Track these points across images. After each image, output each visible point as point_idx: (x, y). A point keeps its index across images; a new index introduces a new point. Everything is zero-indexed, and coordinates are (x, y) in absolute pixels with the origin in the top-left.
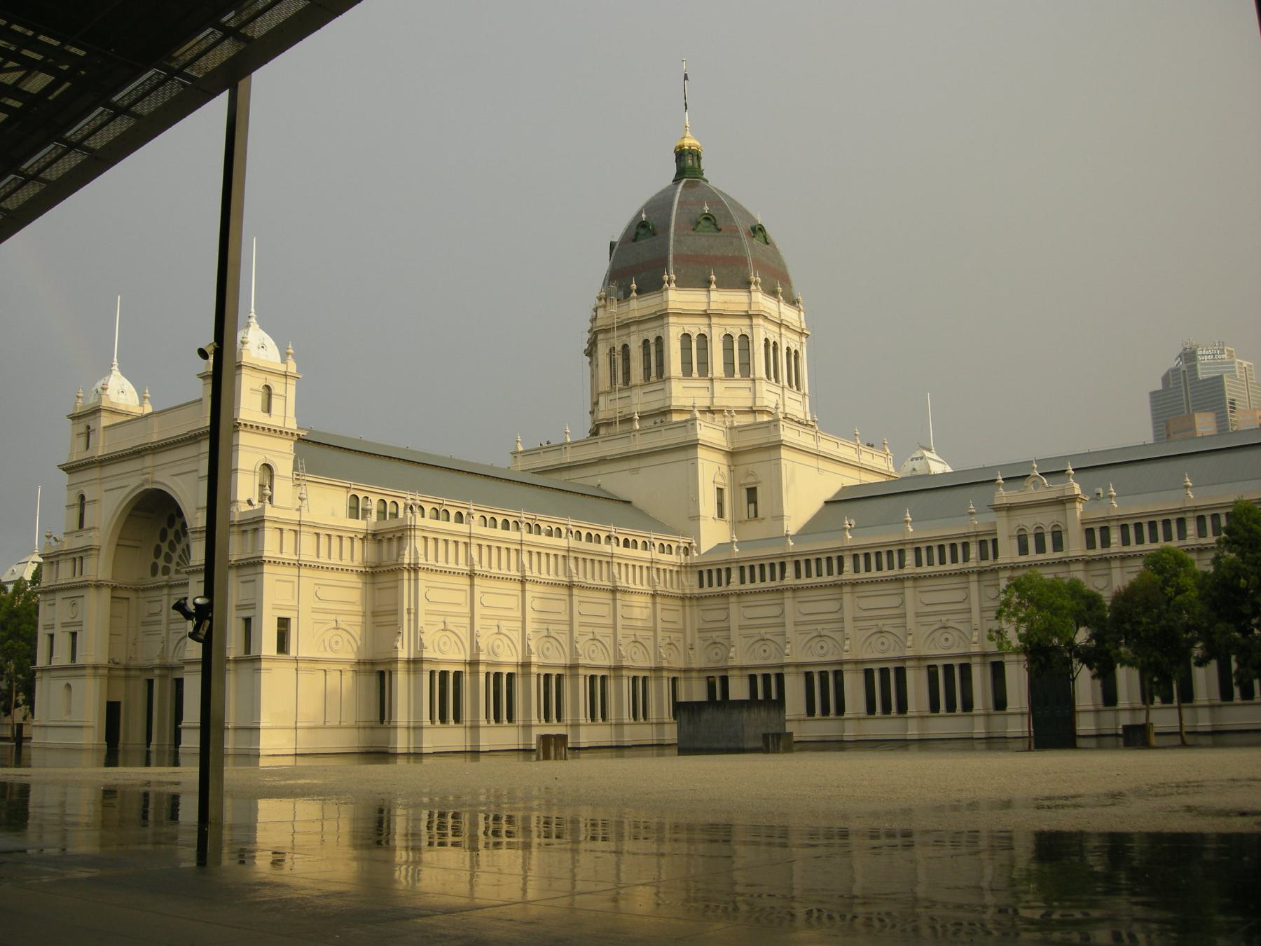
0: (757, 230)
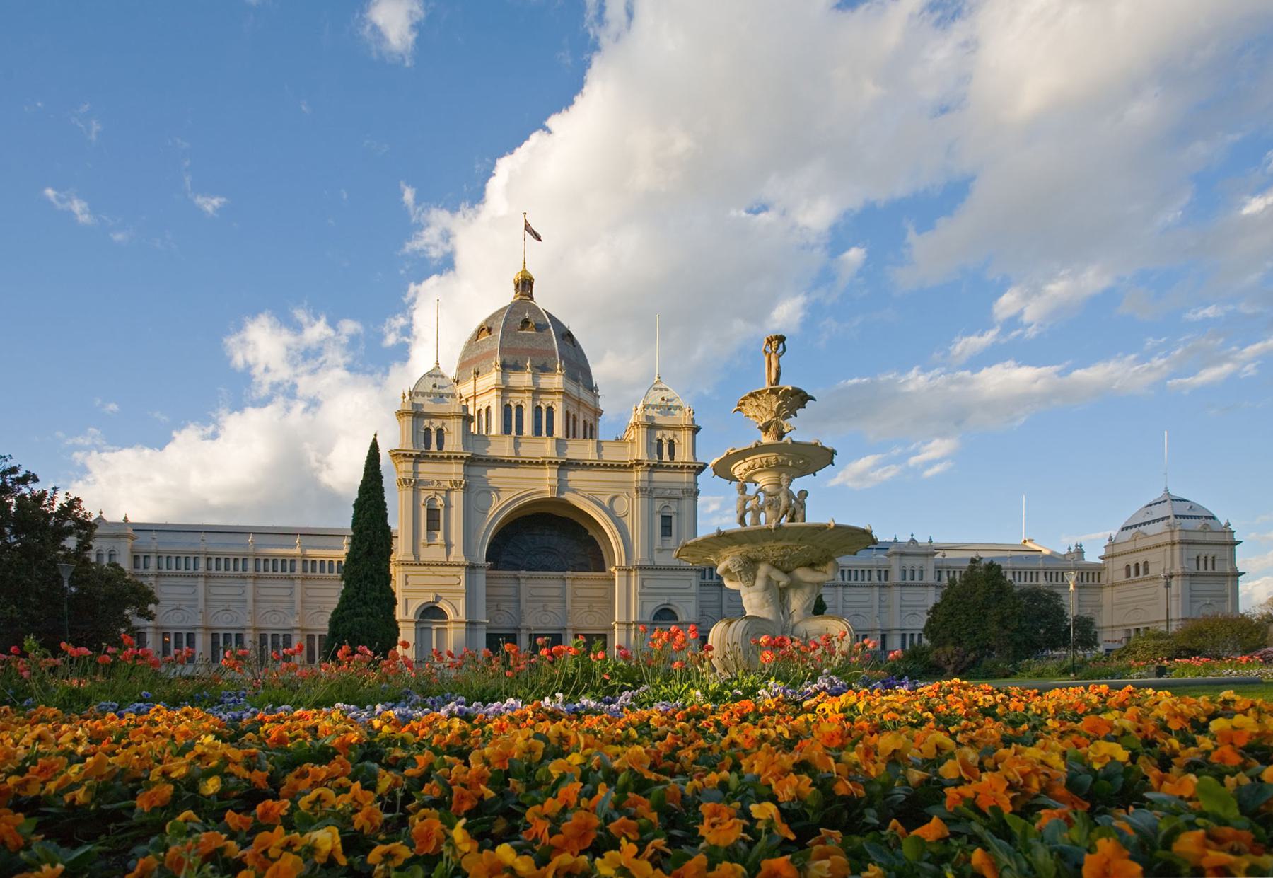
0: (566, 336)
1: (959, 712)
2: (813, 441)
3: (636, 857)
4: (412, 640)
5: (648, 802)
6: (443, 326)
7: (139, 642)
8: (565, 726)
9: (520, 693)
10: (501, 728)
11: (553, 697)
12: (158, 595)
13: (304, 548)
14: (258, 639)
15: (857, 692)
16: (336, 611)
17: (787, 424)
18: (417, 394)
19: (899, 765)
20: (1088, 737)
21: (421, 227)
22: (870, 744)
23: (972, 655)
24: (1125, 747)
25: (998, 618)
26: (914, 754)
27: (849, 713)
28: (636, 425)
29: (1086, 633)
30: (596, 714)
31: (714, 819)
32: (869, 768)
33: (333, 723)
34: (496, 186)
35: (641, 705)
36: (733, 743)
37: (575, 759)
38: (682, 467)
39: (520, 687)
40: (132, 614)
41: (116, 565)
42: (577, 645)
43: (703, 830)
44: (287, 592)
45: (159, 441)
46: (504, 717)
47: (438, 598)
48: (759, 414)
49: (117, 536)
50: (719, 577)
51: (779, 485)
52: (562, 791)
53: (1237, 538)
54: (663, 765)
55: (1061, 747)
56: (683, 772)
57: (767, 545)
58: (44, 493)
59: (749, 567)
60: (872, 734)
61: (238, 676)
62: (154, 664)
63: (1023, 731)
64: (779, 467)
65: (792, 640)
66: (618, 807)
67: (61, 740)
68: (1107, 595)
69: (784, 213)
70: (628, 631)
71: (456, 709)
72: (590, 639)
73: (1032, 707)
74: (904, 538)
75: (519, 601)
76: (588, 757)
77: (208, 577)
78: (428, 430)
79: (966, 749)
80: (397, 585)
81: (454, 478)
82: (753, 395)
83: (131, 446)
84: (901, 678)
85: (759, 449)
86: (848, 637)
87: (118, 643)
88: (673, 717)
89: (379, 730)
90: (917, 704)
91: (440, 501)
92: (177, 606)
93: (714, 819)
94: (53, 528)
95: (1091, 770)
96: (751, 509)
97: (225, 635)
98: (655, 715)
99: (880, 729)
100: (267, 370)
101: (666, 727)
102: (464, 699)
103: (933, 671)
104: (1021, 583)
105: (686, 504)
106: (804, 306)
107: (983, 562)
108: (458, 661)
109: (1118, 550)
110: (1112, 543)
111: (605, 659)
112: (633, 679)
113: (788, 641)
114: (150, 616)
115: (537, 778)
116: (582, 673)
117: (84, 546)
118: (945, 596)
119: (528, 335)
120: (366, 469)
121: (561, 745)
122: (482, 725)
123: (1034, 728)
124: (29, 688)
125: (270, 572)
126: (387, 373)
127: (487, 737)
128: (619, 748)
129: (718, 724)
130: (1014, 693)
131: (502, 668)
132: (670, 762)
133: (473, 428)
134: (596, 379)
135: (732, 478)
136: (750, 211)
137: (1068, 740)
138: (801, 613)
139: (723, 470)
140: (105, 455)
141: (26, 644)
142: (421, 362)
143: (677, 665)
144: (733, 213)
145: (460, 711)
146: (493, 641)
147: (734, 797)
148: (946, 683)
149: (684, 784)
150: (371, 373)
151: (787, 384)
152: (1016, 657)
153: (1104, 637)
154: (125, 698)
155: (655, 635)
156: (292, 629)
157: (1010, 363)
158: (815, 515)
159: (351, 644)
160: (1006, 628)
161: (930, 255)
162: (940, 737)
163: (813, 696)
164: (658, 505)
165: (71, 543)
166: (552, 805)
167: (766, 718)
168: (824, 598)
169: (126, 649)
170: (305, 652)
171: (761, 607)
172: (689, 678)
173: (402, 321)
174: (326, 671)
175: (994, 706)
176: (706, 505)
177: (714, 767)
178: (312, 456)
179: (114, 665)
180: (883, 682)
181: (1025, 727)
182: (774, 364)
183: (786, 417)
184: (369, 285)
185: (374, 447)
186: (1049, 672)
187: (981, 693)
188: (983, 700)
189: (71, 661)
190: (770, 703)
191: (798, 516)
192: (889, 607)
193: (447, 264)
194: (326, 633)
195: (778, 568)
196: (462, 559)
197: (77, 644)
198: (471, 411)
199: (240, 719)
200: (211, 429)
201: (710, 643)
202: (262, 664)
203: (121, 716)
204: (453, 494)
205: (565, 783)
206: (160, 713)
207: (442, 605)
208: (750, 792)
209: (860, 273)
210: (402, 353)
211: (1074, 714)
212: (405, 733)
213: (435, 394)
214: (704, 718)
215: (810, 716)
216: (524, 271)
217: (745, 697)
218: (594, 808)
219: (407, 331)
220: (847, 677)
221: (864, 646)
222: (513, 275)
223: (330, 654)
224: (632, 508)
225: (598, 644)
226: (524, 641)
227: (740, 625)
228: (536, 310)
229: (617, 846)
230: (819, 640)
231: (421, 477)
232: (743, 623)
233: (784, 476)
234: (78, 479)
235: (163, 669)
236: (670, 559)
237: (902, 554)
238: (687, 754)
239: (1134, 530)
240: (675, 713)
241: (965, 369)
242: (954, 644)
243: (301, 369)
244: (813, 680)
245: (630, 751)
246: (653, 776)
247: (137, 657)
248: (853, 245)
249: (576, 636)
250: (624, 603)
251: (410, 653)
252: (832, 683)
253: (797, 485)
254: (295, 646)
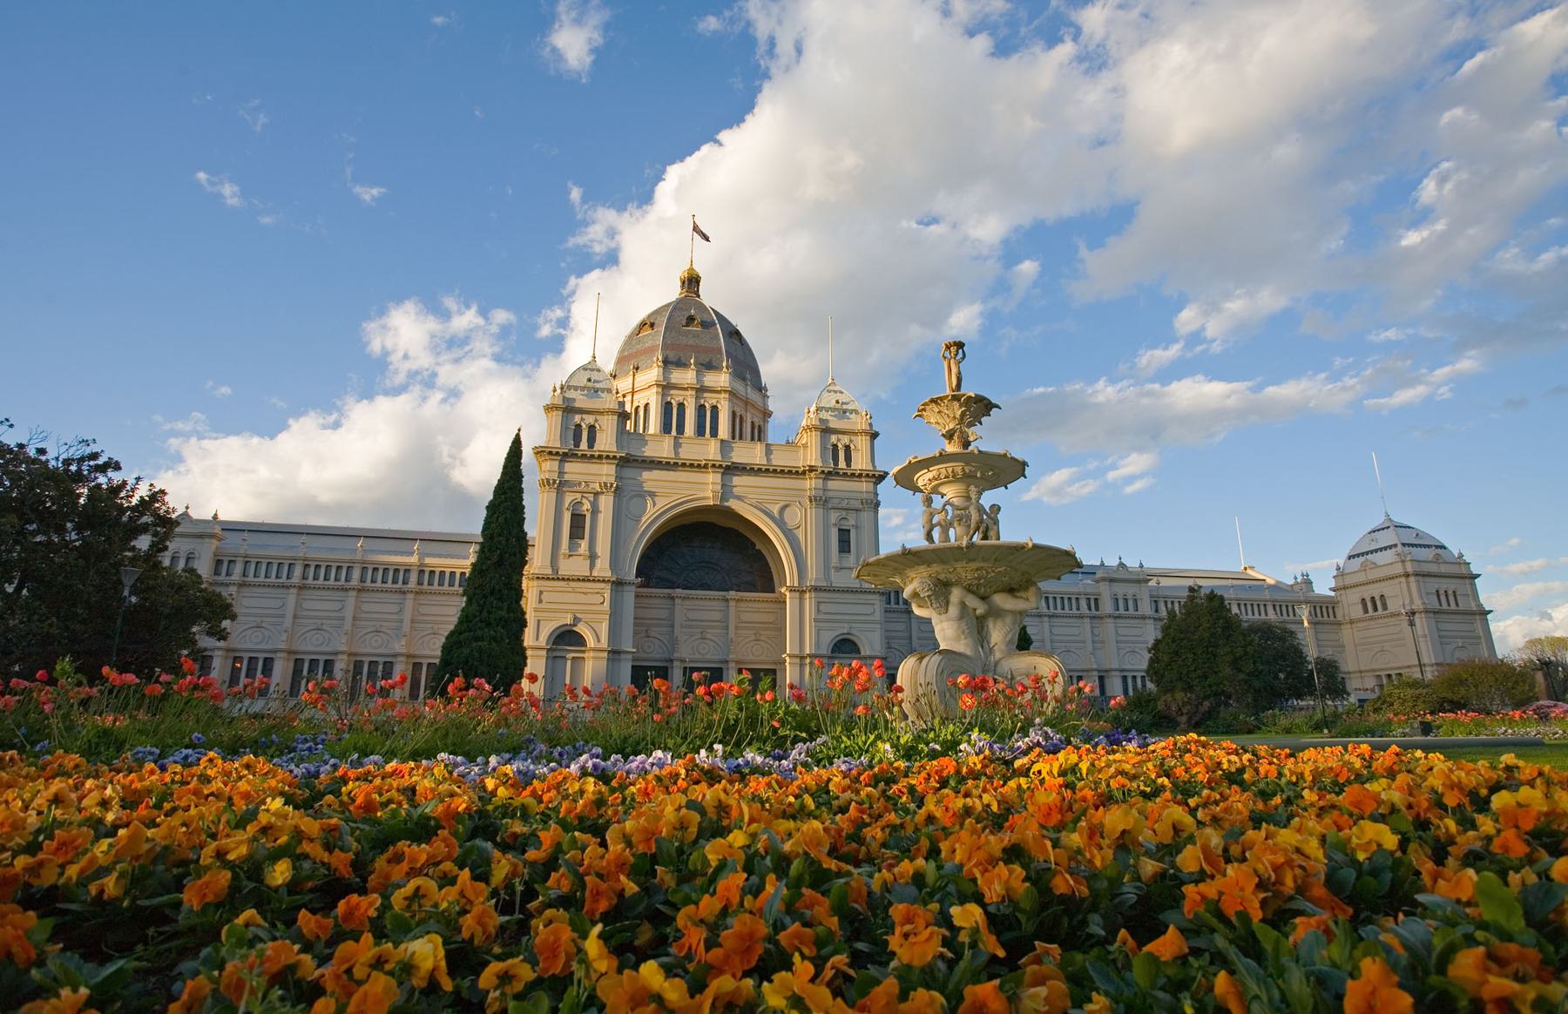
1: (1200, 777)
2: (1002, 452)
3: (812, 980)
4: (540, 672)
5: (827, 902)
6: (602, 321)
7: (202, 668)
8: (725, 791)
9: (670, 743)
10: (646, 793)
11: (710, 749)
12: (237, 609)
13: (422, 556)
14: (351, 667)
15: (1078, 748)
16: (452, 633)
17: (973, 432)
18: (569, 388)
19: (1128, 851)
20: (1351, 815)
21: (586, 223)
22: (1095, 821)
23: (1207, 704)
24: (1395, 831)
25: (1229, 658)
26: (1146, 837)
27: (1070, 778)
28: (809, 428)
29: (1332, 681)
30: (763, 775)
31: (908, 928)
32: (1093, 856)
33: (435, 782)
34: (665, 190)
35: (818, 763)
36: (930, 819)
37: (738, 838)
38: (860, 475)
39: (670, 736)
40: (200, 632)
41: (192, 571)
42: (741, 682)
43: (894, 942)
44: (395, 608)
45: (271, 428)
46: (650, 777)
47: (576, 620)
48: (943, 420)
49: (201, 536)
50: (906, 602)
51: (968, 498)
52: (721, 884)
53: (1474, 570)
54: (845, 849)
55: (1319, 829)
56: (870, 860)
57: (958, 565)
58: (125, 483)
59: (941, 590)
60: (1097, 808)
61: (320, 715)
62: (215, 697)
63: (1277, 803)
64: (967, 478)
65: (995, 681)
66: (790, 908)
67: (85, 803)
68: (1347, 634)
69: (954, 226)
70: (802, 666)
71: (590, 764)
72: (757, 675)
73: (1286, 772)
74: (1112, 562)
75: (672, 626)
76: (754, 836)
77: (302, 588)
78: (579, 426)
79: (1208, 831)
80: (529, 603)
81: (604, 479)
82: (933, 401)
83: (237, 433)
84: (1127, 731)
85: (943, 458)
86: (1060, 679)
87: (176, 670)
88: (857, 780)
89: (494, 793)
90: (1150, 765)
91: (587, 506)
92: (259, 624)
93: (908, 928)
94: (125, 525)
95: (1354, 862)
96: (939, 524)
97: (312, 661)
98: (835, 775)
99: (1106, 800)
100: (406, 357)
101: (848, 795)
102: (600, 750)
103: (1163, 724)
104: (1249, 617)
105: (866, 516)
106: (982, 314)
107: (1203, 592)
108: (596, 701)
109: (1349, 581)
110: (1340, 573)
111: (775, 700)
112: (808, 727)
113: (991, 682)
114: (222, 635)
115: (691, 866)
116: (747, 718)
117: (158, 547)
118: (1166, 630)
119: (692, 332)
120: (505, 467)
121: (720, 819)
122: (623, 787)
123: (1288, 802)
124: (48, 726)
125: (379, 584)
126: (538, 365)
127: (629, 805)
128: (791, 824)
129: (912, 790)
130: (1262, 753)
131: (650, 711)
132: (854, 845)
133: (629, 426)
134: (765, 378)
135: (916, 489)
136: (920, 223)
137: (1328, 820)
138: (1003, 647)
139: (906, 479)
140: (205, 443)
141: (58, 667)
142: (576, 354)
143: (860, 710)
144: (904, 224)
145: (595, 766)
146: (640, 676)
147: (931, 895)
148: (1181, 739)
149: (871, 876)
150: (521, 364)
151: (969, 390)
152: (1257, 709)
153: (1352, 685)
154: (170, 741)
155: (834, 671)
156: (395, 656)
157: (1199, 377)
158: (1011, 532)
159: (465, 676)
160: (1240, 671)
161: (1105, 270)
162: (1178, 813)
163: (1025, 753)
164: (834, 516)
165: (143, 543)
166: (709, 905)
167: (970, 782)
168: (1029, 631)
169: (184, 676)
170: (407, 685)
171: (957, 639)
172: (875, 728)
173: (559, 313)
174: (431, 710)
175: (1241, 770)
176: (889, 518)
177: (907, 853)
178: (445, 450)
179: (165, 697)
180: (1107, 736)
181: (1277, 800)
182: (954, 370)
183: (971, 425)
184: (526, 279)
185: (517, 444)
186: (1298, 727)
187: (1224, 753)
188: (1229, 762)
189: (111, 692)
190: (975, 761)
191: (992, 533)
192: (1102, 642)
193: (611, 259)
194: (437, 661)
195: (973, 593)
196: (608, 574)
197: (123, 669)
198: (628, 408)
199: (317, 775)
200: (334, 417)
201: (899, 683)
202: (352, 700)
203: (163, 769)
204: (602, 498)
205: (724, 874)
206: (212, 764)
207: (581, 629)
208: (951, 888)
209: (1035, 284)
210: (556, 345)
211: (1335, 783)
212: (525, 798)
213: (589, 389)
214: (896, 782)
215: (1023, 780)
216: (691, 269)
217: (944, 754)
218: (761, 909)
219: (564, 323)
220: (1064, 730)
221: (1080, 690)
222: (679, 272)
223: (438, 689)
224: (804, 518)
225: (767, 681)
226: (677, 676)
227: (933, 661)
228: (702, 307)
229: (788, 966)
230: (1027, 682)
231: (567, 477)
232: (937, 658)
233: (972, 488)
234: (168, 469)
235: (226, 704)
236: (849, 579)
237: (1112, 580)
238: (875, 833)
239: (1362, 559)
240: (860, 774)
241: (1153, 381)
242: (1184, 690)
243: (443, 358)
244: (1024, 732)
245: (805, 827)
246: (832, 864)
247: (196, 687)
248: (1028, 257)
249: (740, 671)
250: (798, 630)
251: (538, 689)
252: (1046, 736)
253: (988, 499)
254: (396, 677)
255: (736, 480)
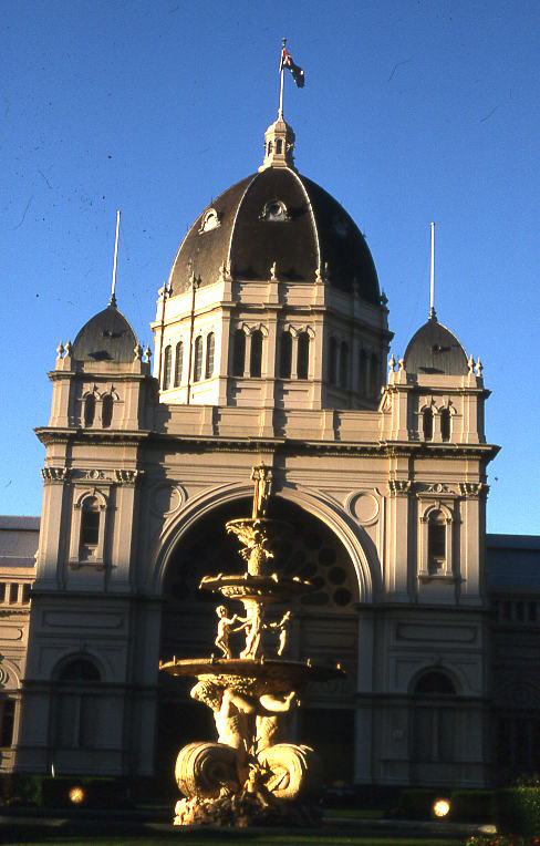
204: (120, 491)
231: (75, 465)
255: (290, 462)
